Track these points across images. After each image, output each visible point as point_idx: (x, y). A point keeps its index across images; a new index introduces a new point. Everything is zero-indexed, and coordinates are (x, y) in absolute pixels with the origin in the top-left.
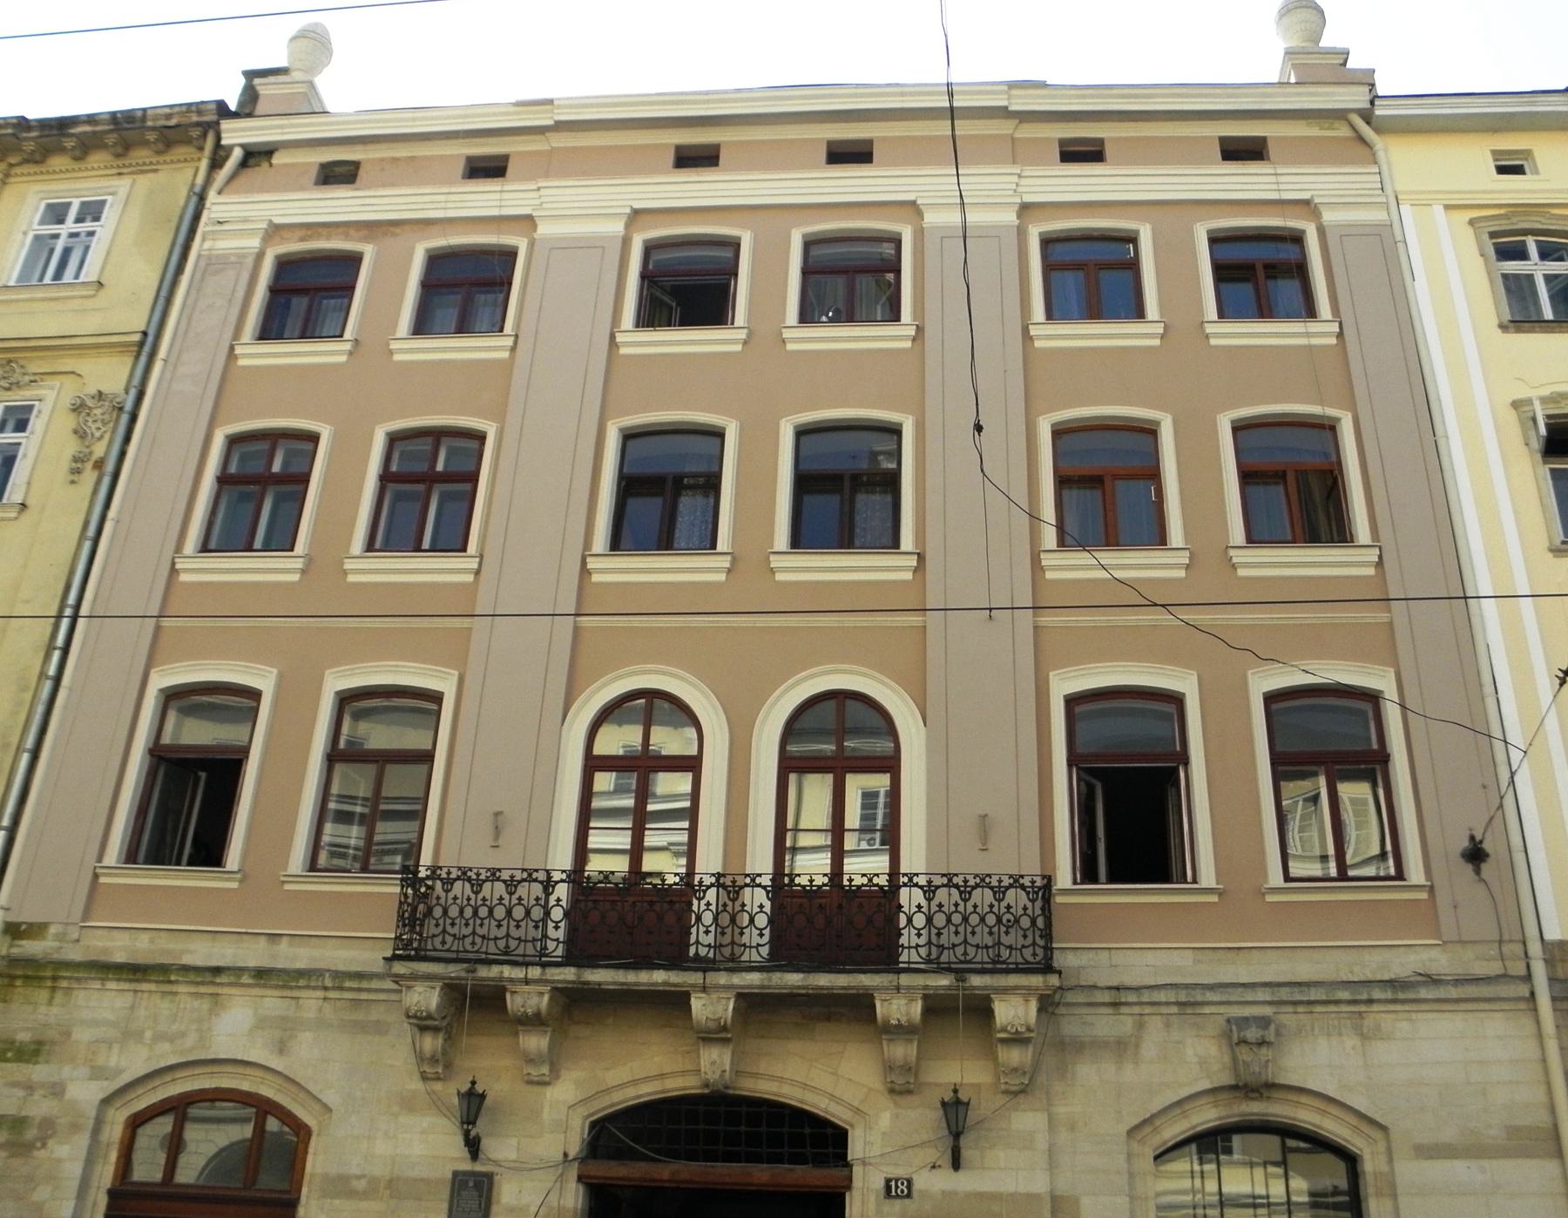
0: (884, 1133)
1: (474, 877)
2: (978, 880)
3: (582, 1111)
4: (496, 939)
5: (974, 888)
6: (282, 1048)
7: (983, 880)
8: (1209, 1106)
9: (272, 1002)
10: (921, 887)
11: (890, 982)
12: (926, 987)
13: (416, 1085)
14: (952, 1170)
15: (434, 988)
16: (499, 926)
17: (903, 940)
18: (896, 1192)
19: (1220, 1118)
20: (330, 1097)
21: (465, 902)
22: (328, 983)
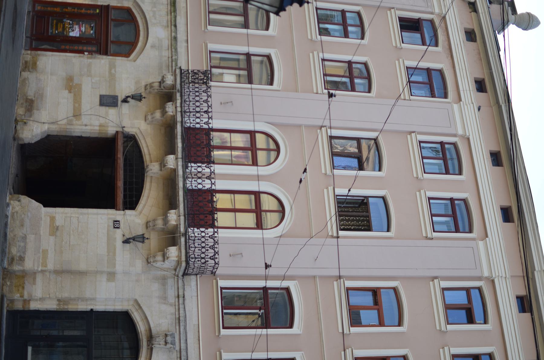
0: (134, 220)
1: (208, 91)
3: (138, 132)
4: (189, 98)
6: (153, 47)
7: (216, 242)
9: (166, 43)
11: (181, 214)
12: (180, 224)
13: (143, 84)
14: (122, 241)
15: (173, 82)
16: (193, 99)
17: (196, 230)
18: (115, 224)
19: (141, 332)
20: (139, 61)
21: (200, 89)
22: (174, 58)
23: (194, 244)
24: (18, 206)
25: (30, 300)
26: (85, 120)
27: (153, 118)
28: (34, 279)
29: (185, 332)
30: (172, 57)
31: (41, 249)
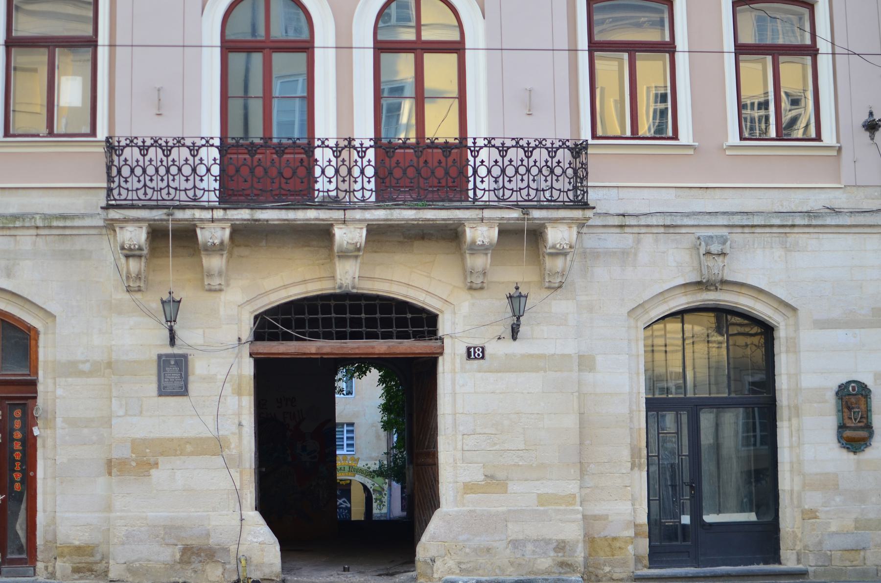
1: (164, 144)
2: (537, 143)
4: (186, 190)
5: (534, 148)
7: (540, 143)
8: (681, 294)
10: (497, 148)
11: (477, 215)
12: (502, 219)
16: (187, 180)
18: (474, 355)
19: (688, 303)
21: (159, 164)
22: (40, 223)
23: (543, 190)
24: (445, 562)
25: (636, 526)
26: (228, 429)
27: (220, 274)
28: (596, 518)
29: (695, 217)
30: (37, 228)
31: (537, 508)
